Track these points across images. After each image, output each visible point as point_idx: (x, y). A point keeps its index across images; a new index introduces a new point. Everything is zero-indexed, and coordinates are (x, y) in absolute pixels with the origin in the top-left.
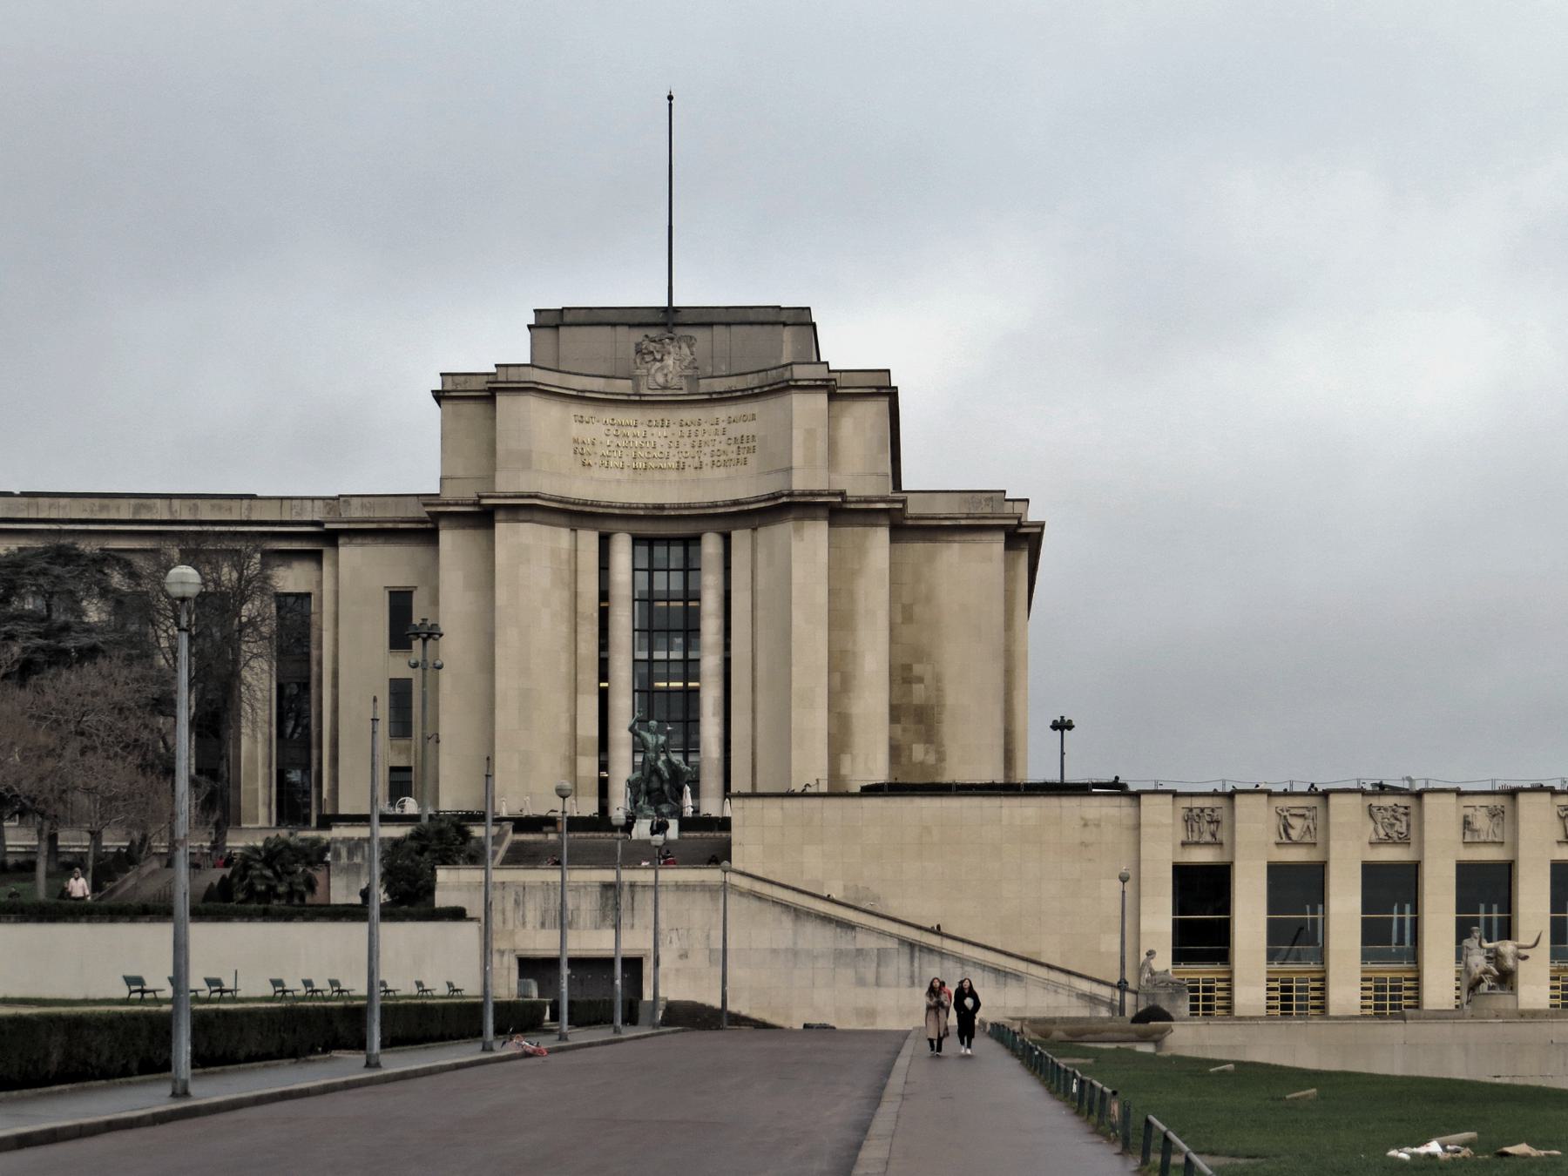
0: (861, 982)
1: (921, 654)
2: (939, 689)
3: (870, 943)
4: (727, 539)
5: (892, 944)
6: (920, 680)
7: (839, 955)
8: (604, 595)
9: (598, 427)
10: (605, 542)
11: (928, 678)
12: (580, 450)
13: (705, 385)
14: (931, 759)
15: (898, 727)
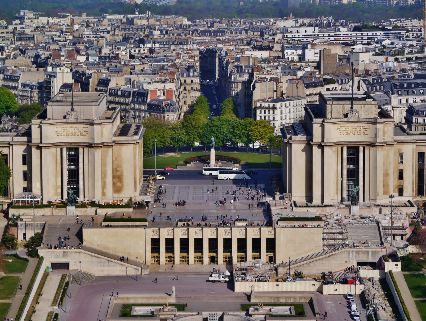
0: (101, 266)
1: (119, 166)
2: (122, 173)
3: (103, 260)
4: (83, 148)
5: (106, 261)
6: (119, 171)
7: (98, 262)
8: (62, 183)
9: (60, 129)
10: (62, 149)
11: (120, 170)
12: (57, 133)
13: (79, 121)
14: (121, 185)
15: (115, 180)
